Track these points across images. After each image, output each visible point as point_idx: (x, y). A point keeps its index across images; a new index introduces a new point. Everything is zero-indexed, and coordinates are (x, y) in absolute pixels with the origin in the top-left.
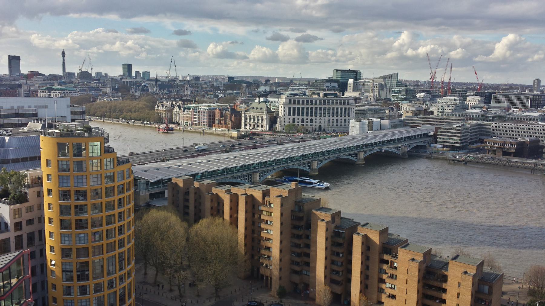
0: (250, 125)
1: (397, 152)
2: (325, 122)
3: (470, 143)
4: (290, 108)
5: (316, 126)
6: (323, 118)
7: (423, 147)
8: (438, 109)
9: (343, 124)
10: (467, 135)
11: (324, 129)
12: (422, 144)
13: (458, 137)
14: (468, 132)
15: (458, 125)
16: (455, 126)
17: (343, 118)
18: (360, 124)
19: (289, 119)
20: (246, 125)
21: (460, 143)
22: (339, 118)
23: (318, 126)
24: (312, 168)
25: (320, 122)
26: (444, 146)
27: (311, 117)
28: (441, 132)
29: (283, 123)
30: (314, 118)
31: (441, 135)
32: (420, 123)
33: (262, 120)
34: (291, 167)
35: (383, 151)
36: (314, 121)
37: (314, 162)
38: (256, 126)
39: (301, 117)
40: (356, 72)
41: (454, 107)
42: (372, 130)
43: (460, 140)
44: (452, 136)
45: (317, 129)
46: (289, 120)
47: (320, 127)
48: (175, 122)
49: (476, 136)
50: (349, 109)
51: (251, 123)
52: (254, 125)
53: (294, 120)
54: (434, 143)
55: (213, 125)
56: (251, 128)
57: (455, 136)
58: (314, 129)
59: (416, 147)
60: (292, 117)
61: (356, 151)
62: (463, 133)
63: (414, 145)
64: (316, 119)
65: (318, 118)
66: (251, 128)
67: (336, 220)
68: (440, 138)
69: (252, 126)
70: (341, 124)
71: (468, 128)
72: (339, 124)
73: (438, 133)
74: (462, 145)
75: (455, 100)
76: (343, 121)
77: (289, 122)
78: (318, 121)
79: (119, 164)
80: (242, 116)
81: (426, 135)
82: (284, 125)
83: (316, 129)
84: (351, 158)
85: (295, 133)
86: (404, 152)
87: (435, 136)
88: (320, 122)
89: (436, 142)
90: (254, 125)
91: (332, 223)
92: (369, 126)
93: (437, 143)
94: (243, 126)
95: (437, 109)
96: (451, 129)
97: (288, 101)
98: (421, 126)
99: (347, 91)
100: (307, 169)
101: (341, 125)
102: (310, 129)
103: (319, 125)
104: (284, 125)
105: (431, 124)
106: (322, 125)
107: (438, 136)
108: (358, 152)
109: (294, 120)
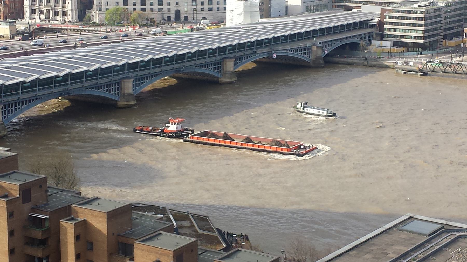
0: (41, 12)
1: (304, 58)
3: (445, 37)
5: (169, 10)
7: (354, 47)
10: (439, 22)
11: (186, 18)
13: (420, 25)
14: (439, 16)
16: (416, 6)
18: (245, 6)
20: (33, 12)
21: (425, 38)
23: (173, 11)
24: (124, 94)
26: (396, 44)
28: (392, 17)
29: (104, 7)
31: (392, 24)
34: (76, 93)
35: (275, 56)
37: (125, 80)
38: (52, 13)
42: (269, 16)
43: (425, 32)
44: (409, 25)
47: (178, 13)
49: (457, 24)
52: (49, 12)
54: (379, 38)
56: (43, 17)
57: (415, 25)
58: (166, 17)
61: (218, 58)
62: (431, 18)
63: (339, 44)
66: (43, 17)
67: (33, 195)
68: (389, 30)
69: (45, 12)
70: (218, 6)
71: (439, 9)
73: (385, 20)
74: (427, 40)
81: (364, 24)
82: (107, 9)
83: (169, 18)
85: (124, 26)
86: (317, 58)
87: (381, 24)
89: (382, 37)
90: (49, 12)
91: (24, 203)
92: (261, 10)
93: (385, 38)
94: (27, 13)
96: (410, 12)
100: (111, 95)
101: (218, 9)
102: (157, 18)
103: (176, 9)
107: (385, 26)
108: (223, 59)
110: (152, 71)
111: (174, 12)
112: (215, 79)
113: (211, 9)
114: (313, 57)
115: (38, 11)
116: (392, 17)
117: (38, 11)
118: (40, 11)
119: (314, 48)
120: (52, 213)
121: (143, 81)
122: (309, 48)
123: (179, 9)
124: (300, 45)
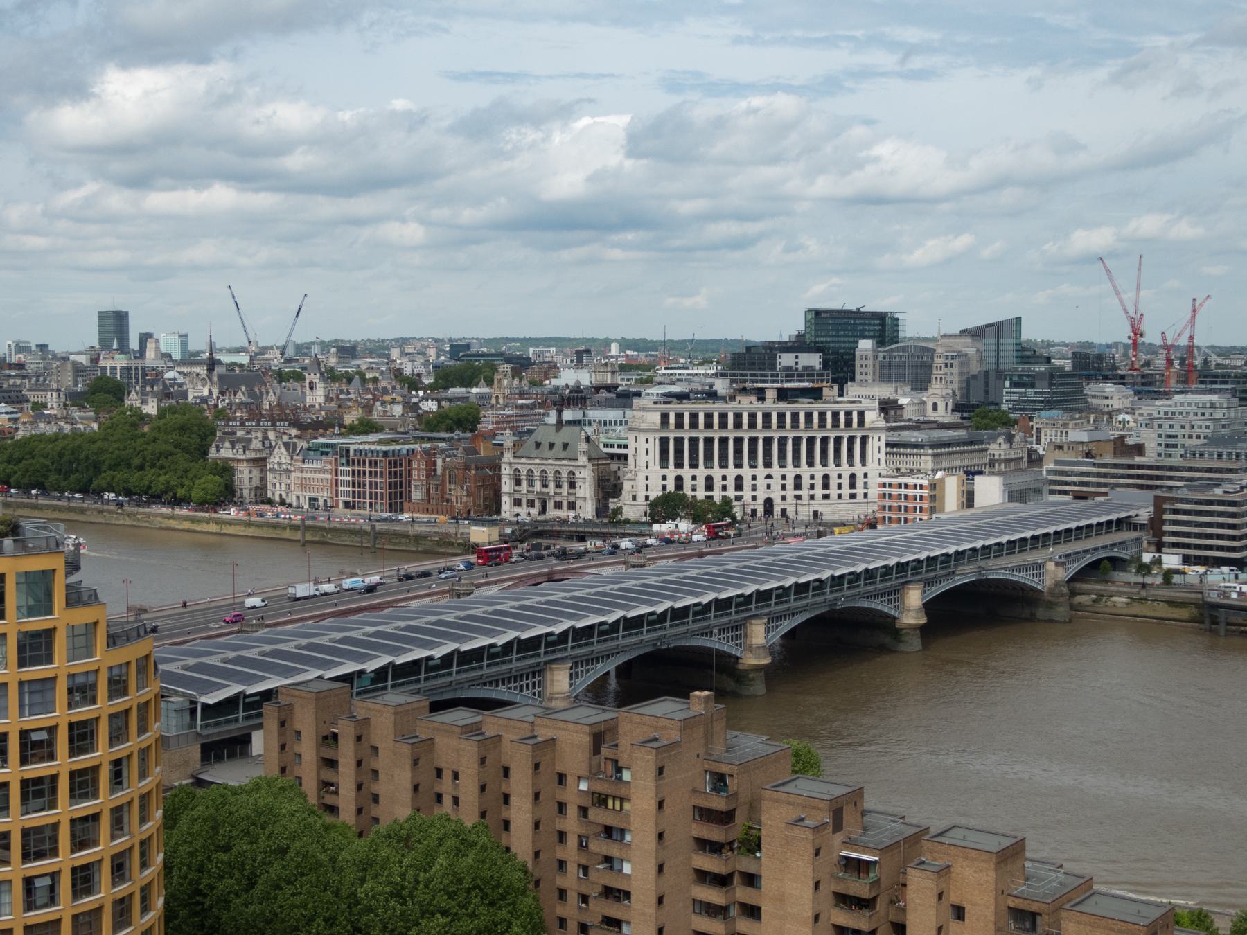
0: (531, 503)
2: (784, 487)
4: (664, 442)
5: (754, 498)
6: (776, 470)
8: (1160, 436)
9: (846, 491)
11: (784, 512)
12: (1116, 553)
15: (1229, 488)
16: (1219, 491)
17: (846, 470)
19: (664, 478)
20: (517, 503)
22: (832, 470)
23: (761, 500)
24: (751, 646)
25: (769, 486)
26: (1186, 560)
27: (739, 472)
28: (1176, 512)
29: (641, 494)
30: (746, 472)
32: (1105, 485)
33: (572, 485)
36: (747, 483)
37: (753, 621)
38: (550, 505)
39: (701, 472)
40: (881, 317)
41: (1212, 427)
45: (760, 510)
46: (664, 483)
47: (769, 503)
48: (277, 498)
50: (864, 440)
51: (531, 497)
53: (679, 480)
55: (406, 505)
58: (749, 511)
59: (1095, 566)
60: (672, 472)
63: (1089, 558)
64: (754, 478)
65: (761, 471)
69: (537, 504)
70: (839, 492)
72: (833, 492)
75: (1212, 405)
76: (845, 482)
77: (664, 488)
78: (761, 482)
79: (115, 644)
80: (503, 471)
82: (647, 498)
83: (754, 512)
84: (879, 608)
86: (1057, 584)
88: (769, 486)
95: (1154, 435)
96: (1210, 503)
97: (657, 418)
98: (1105, 494)
99: (853, 379)
101: (840, 496)
104: (647, 498)
105: (1141, 487)
106: (776, 495)
109: (679, 480)
110: (793, 605)
111: (762, 502)
112: (889, 620)
113: (826, 497)
114: (1049, 582)
115: (524, 501)
116: (1176, 512)
117: (524, 501)
118: (528, 501)
119: (1051, 566)
120: (884, 851)
121: (779, 623)
122: (1042, 566)
123: (772, 496)
124: (1029, 557)
